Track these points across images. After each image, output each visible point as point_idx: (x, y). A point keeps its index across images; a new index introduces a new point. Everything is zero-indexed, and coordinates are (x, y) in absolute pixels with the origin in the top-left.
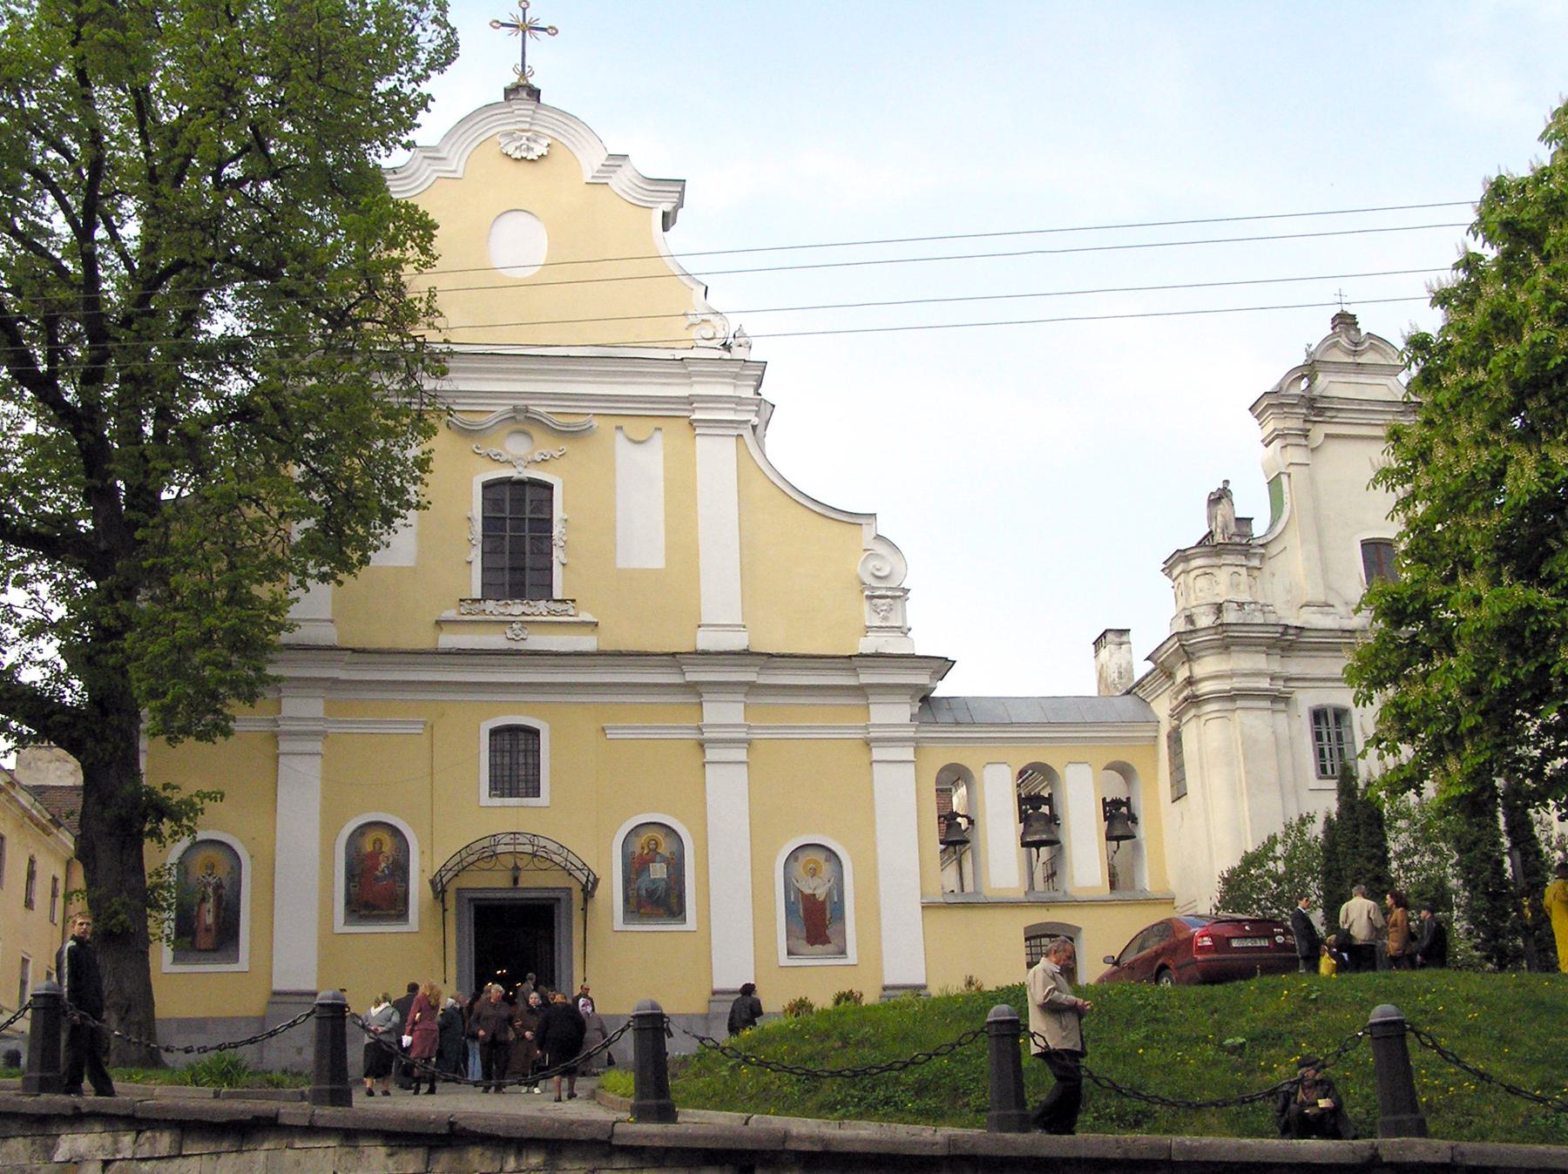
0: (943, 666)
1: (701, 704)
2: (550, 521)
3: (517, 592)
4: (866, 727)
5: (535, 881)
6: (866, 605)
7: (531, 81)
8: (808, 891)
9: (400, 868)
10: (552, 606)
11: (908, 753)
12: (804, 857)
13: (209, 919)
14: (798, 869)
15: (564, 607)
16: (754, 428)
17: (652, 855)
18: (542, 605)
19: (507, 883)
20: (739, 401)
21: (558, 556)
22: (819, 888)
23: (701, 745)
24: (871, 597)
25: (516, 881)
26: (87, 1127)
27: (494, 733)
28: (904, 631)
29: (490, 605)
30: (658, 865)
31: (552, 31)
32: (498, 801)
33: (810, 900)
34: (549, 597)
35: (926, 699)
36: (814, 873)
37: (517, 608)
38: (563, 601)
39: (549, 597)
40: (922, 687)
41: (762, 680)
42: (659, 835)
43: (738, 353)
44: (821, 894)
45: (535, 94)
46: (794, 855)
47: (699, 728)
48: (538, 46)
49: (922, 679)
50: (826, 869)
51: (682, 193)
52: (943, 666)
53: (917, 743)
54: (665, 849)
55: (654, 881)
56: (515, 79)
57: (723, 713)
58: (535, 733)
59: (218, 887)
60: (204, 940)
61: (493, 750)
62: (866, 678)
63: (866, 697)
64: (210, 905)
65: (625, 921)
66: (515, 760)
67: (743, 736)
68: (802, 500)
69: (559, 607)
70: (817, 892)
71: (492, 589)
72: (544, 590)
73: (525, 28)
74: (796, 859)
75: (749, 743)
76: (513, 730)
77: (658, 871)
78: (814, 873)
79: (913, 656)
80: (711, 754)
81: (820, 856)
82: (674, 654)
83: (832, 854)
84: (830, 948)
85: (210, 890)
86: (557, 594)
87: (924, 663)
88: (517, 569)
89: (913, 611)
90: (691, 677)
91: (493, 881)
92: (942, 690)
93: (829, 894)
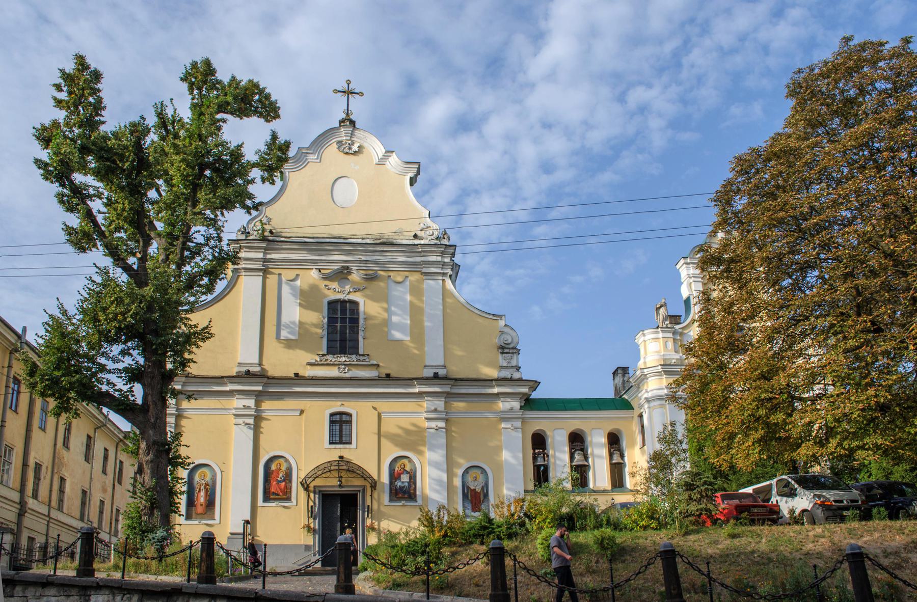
0: (534, 385)
2: (358, 319)
3: (343, 351)
7: (351, 117)
8: (472, 488)
9: (288, 476)
10: (358, 357)
13: (202, 500)
16: (450, 276)
18: (354, 357)
20: (444, 264)
21: (361, 333)
22: (477, 486)
24: (502, 353)
26: (102, 592)
27: (332, 415)
28: (518, 369)
29: (330, 357)
31: (361, 94)
32: (333, 446)
34: (357, 353)
37: (343, 359)
38: (363, 355)
39: (357, 353)
40: (524, 394)
43: (445, 242)
44: (478, 490)
45: (353, 123)
46: (466, 471)
48: (354, 100)
49: (525, 390)
50: (481, 478)
51: (419, 169)
52: (534, 385)
53: (523, 420)
54: (408, 468)
56: (344, 116)
58: (351, 415)
59: (207, 485)
60: (200, 509)
61: (332, 422)
64: (202, 493)
65: (391, 500)
66: (340, 427)
68: (471, 309)
69: (362, 358)
71: (331, 350)
72: (355, 350)
73: (349, 93)
76: (341, 414)
77: (405, 478)
78: (475, 479)
79: (520, 380)
81: (479, 472)
83: (484, 471)
85: (202, 487)
86: (361, 352)
88: (343, 340)
89: (521, 360)
91: (331, 483)
92: (534, 395)
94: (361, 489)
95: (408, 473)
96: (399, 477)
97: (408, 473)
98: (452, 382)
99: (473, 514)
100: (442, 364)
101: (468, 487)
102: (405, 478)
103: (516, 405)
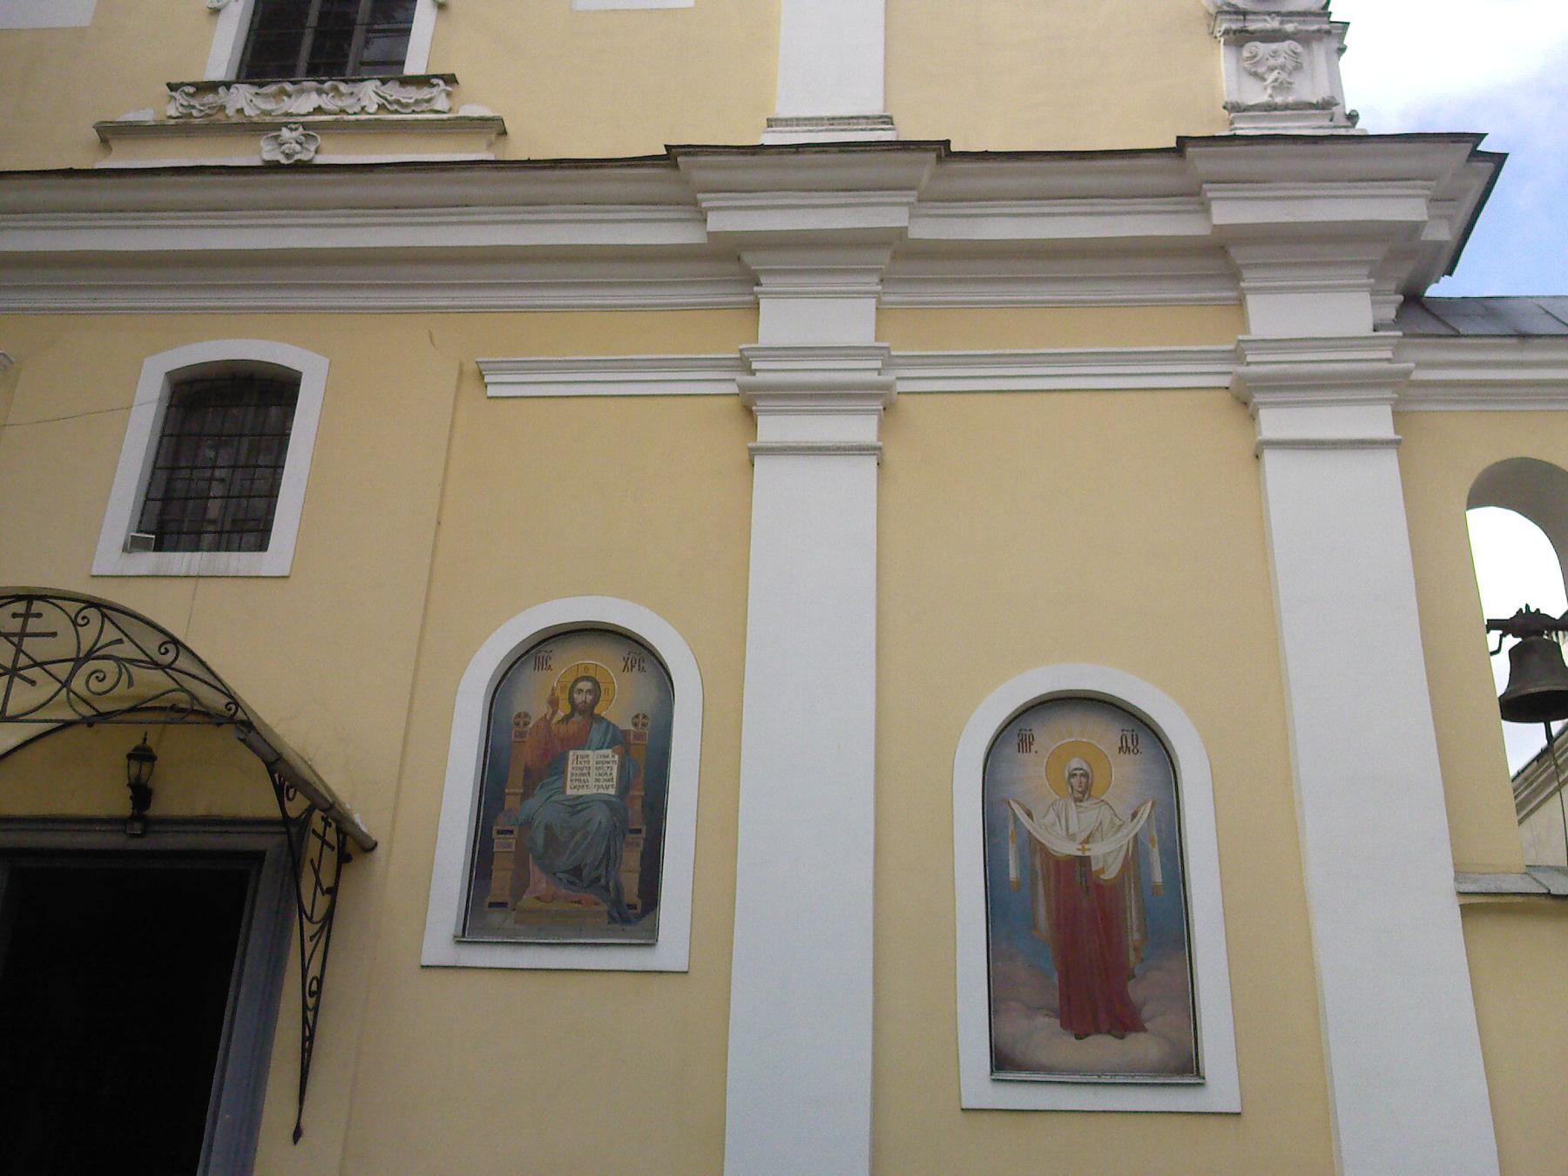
0: (1481, 137)
1: (756, 307)
4: (1237, 356)
5: (211, 789)
6: (1224, 61)
8: (1066, 848)
10: (394, 91)
11: (1376, 421)
12: (1051, 735)
14: (1033, 774)
15: (425, 93)
17: (584, 722)
18: (368, 95)
19: (121, 804)
23: (748, 407)
24: (1239, 38)
25: (141, 794)
29: (244, 100)
30: (593, 755)
32: (148, 561)
33: (1072, 873)
35: (1413, 300)
36: (1083, 788)
37: (304, 101)
38: (423, 81)
41: (927, 230)
42: (604, 661)
44: (1107, 856)
46: (1019, 727)
47: (744, 365)
49: (1403, 208)
50: (1125, 775)
52: (1481, 137)
53: (1403, 393)
54: (622, 703)
55: (578, 806)
57: (813, 321)
62: (1228, 212)
63: (1234, 276)
65: (472, 928)
66: (221, 453)
67: (873, 377)
69: (410, 94)
70: (1096, 851)
74: (1025, 743)
75: (884, 401)
77: (593, 774)
78: (1083, 788)
80: (771, 428)
81: (1103, 735)
82: (672, 156)
83: (1139, 728)
84: (1143, 1047)
86: (413, 67)
87: (1408, 161)
90: (727, 221)
93: (1135, 858)
94: (269, 843)
95: (617, 739)
96: (551, 765)
97: (617, 739)
98: (924, 169)
99: (1068, 1049)
100: (876, 108)
101: (1032, 847)
102: (593, 774)
103: (1346, 312)
